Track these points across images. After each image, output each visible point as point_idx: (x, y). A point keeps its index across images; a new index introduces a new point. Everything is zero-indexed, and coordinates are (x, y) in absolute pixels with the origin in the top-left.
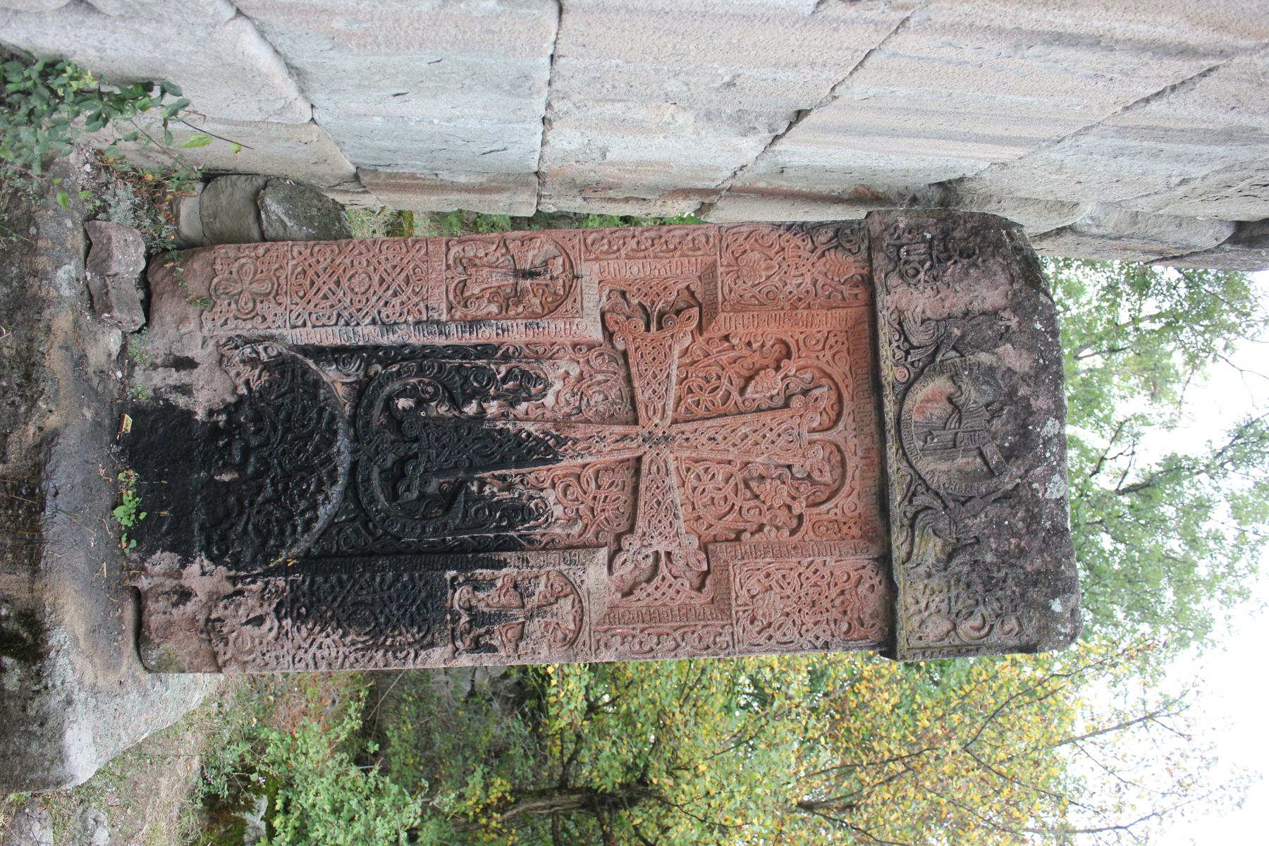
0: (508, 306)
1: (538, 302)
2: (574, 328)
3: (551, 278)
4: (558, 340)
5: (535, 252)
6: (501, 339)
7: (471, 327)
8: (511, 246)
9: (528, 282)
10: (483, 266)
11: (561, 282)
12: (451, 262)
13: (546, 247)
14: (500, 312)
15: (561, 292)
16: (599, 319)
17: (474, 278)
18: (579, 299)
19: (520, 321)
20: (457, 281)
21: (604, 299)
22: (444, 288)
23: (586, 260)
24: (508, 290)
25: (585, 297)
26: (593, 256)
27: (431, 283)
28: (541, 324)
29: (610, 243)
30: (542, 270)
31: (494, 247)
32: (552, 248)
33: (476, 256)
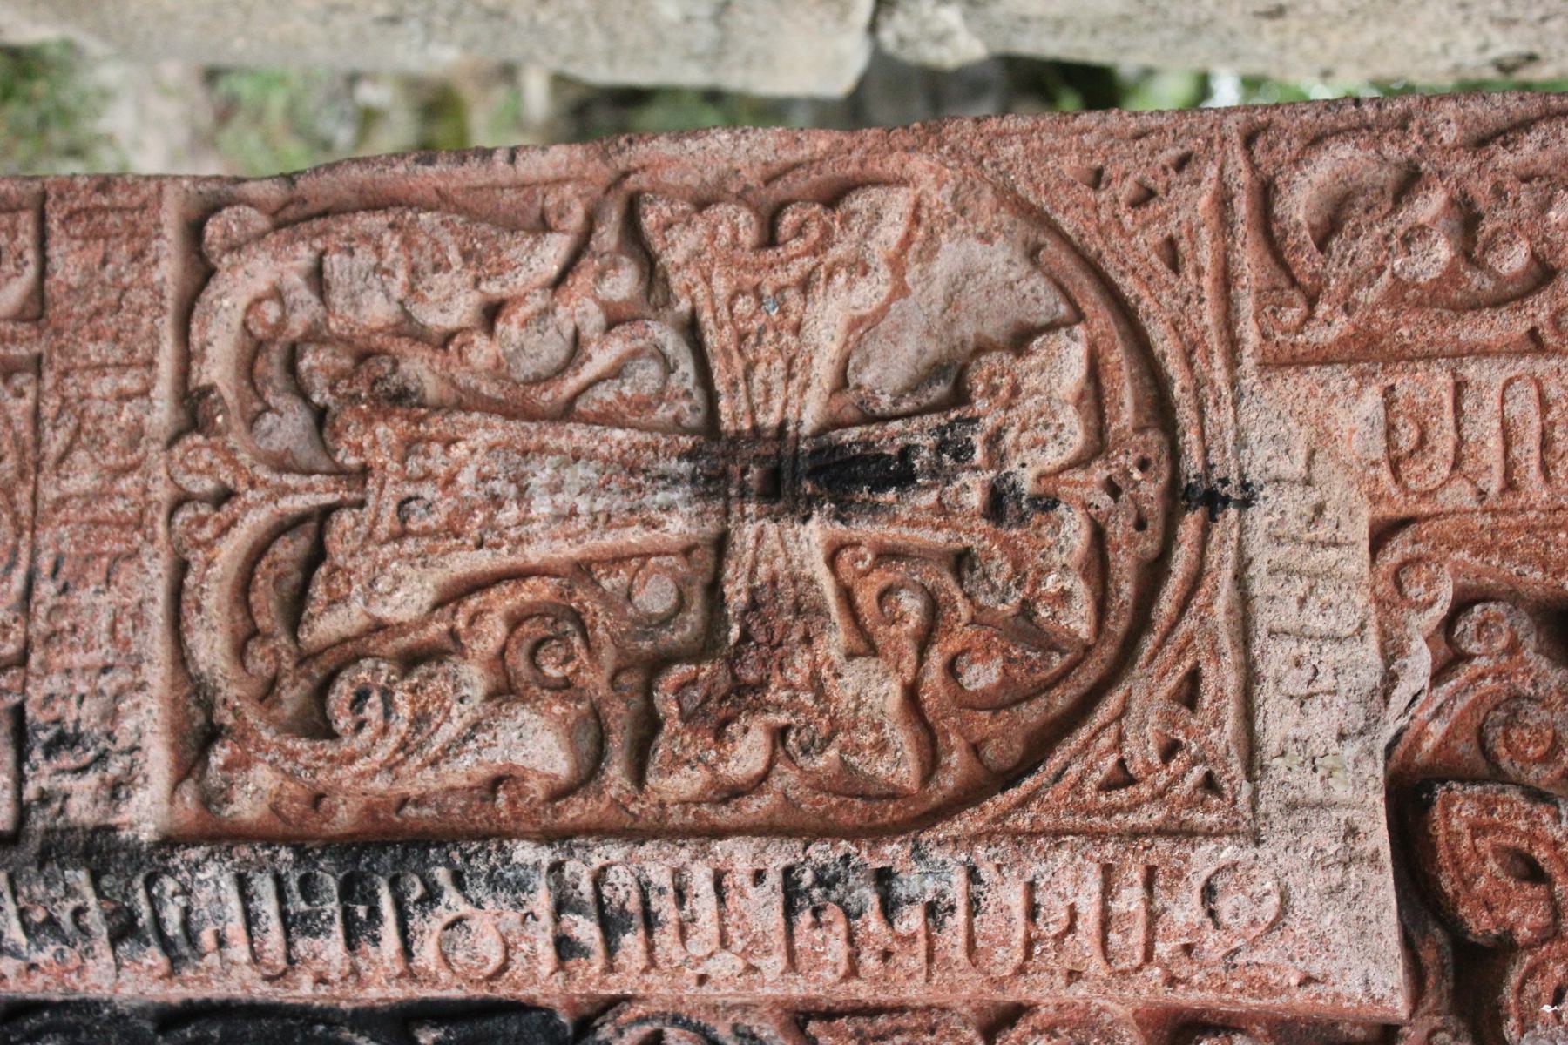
0: (649, 726)
1: (886, 694)
2: (1184, 911)
3: (998, 504)
4: (1044, 992)
5: (869, 293)
6: (590, 978)
7: (354, 889)
8: (677, 249)
9: (815, 533)
10: (467, 401)
11: (1074, 532)
12: (217, 369)
13: (951, 256)
14: (588, 775)
15: (1079, 620)
16: (1379, 838)
17: (384, 502)
18: (1222, 678)
19: (739, 854)
20: (254, 520)
21: (1419, 661)
22: (157, 569)
23: (1277, 362)
24: (655, 596)
25: (1274, 658)
26: (1330, 329)
27: (57, 537)
28: (914, 883)
29: (1466, 217)
30: (921, 436)
31: (552, 252)
32: (1001, 259)
33: (408, 329)
